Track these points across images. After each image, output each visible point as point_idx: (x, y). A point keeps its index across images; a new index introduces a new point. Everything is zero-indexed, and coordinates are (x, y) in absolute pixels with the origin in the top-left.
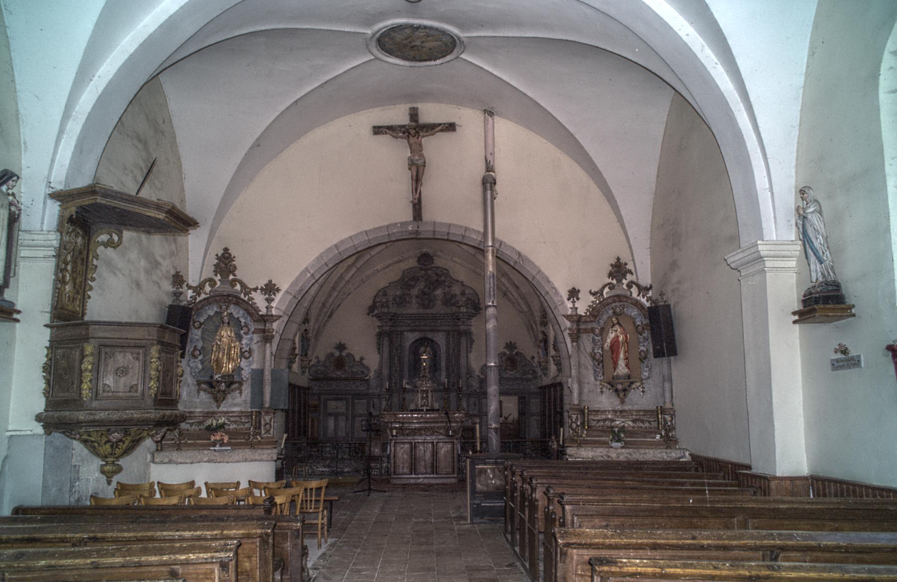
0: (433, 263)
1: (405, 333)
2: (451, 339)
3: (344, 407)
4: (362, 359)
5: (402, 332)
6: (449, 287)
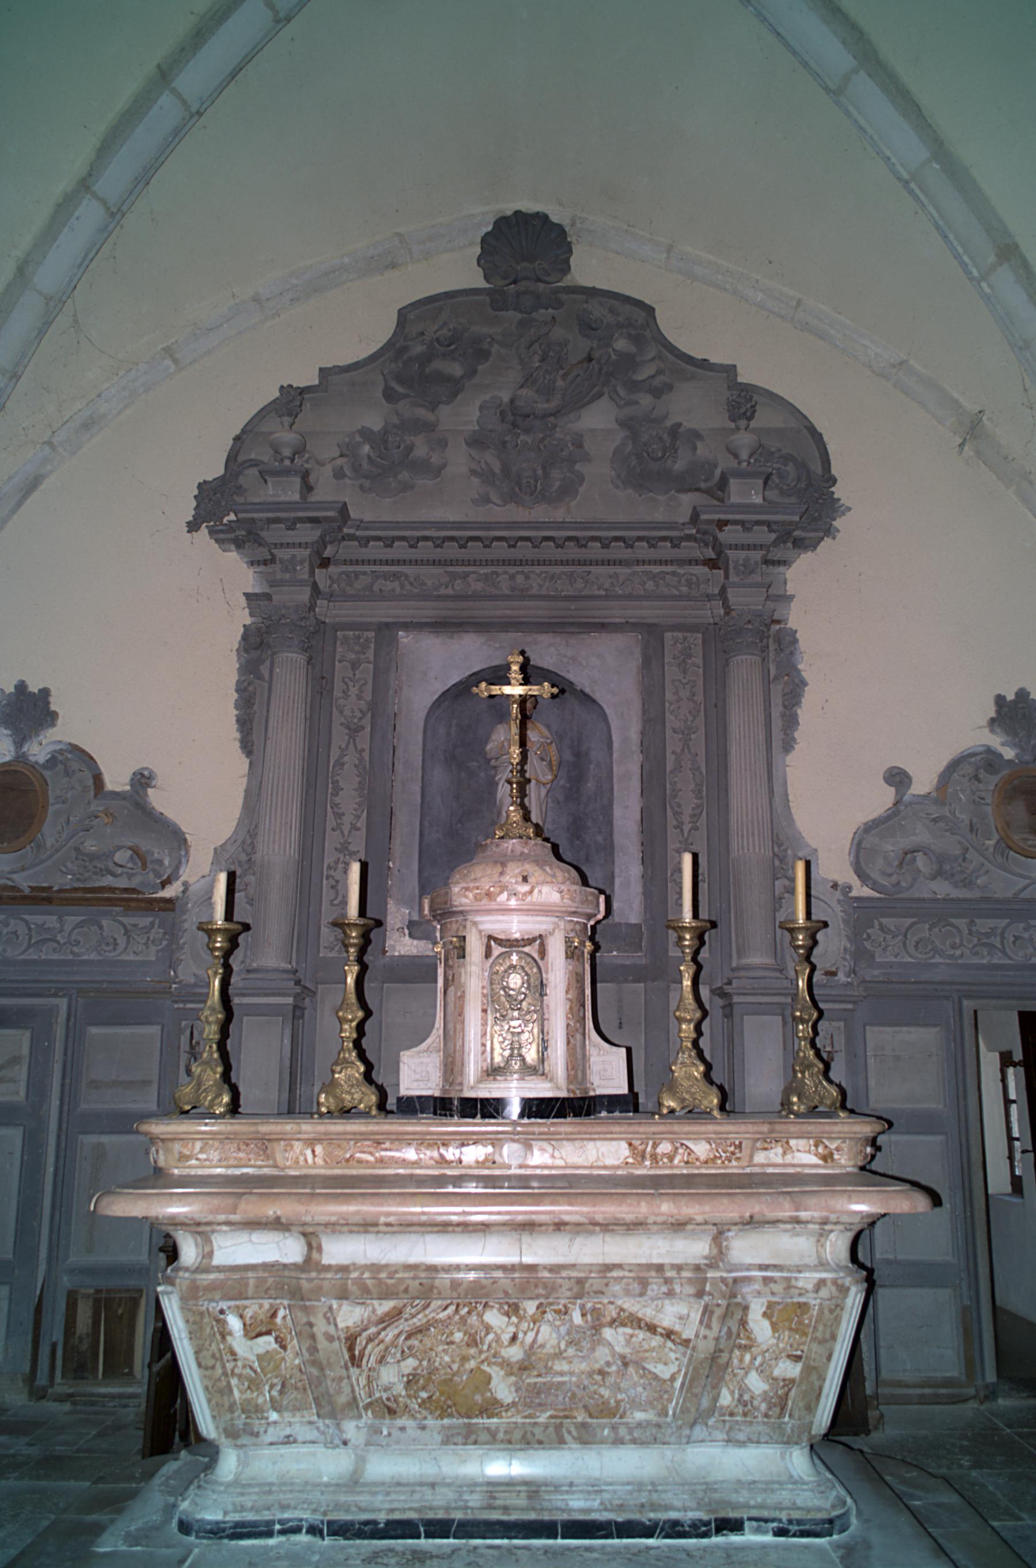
0: (566, 269)
1: (404, 637)
2: (672, 672)
3: (21, 1072)
4: (143, 780)
5: (386, 631)
6: (658, 393)
